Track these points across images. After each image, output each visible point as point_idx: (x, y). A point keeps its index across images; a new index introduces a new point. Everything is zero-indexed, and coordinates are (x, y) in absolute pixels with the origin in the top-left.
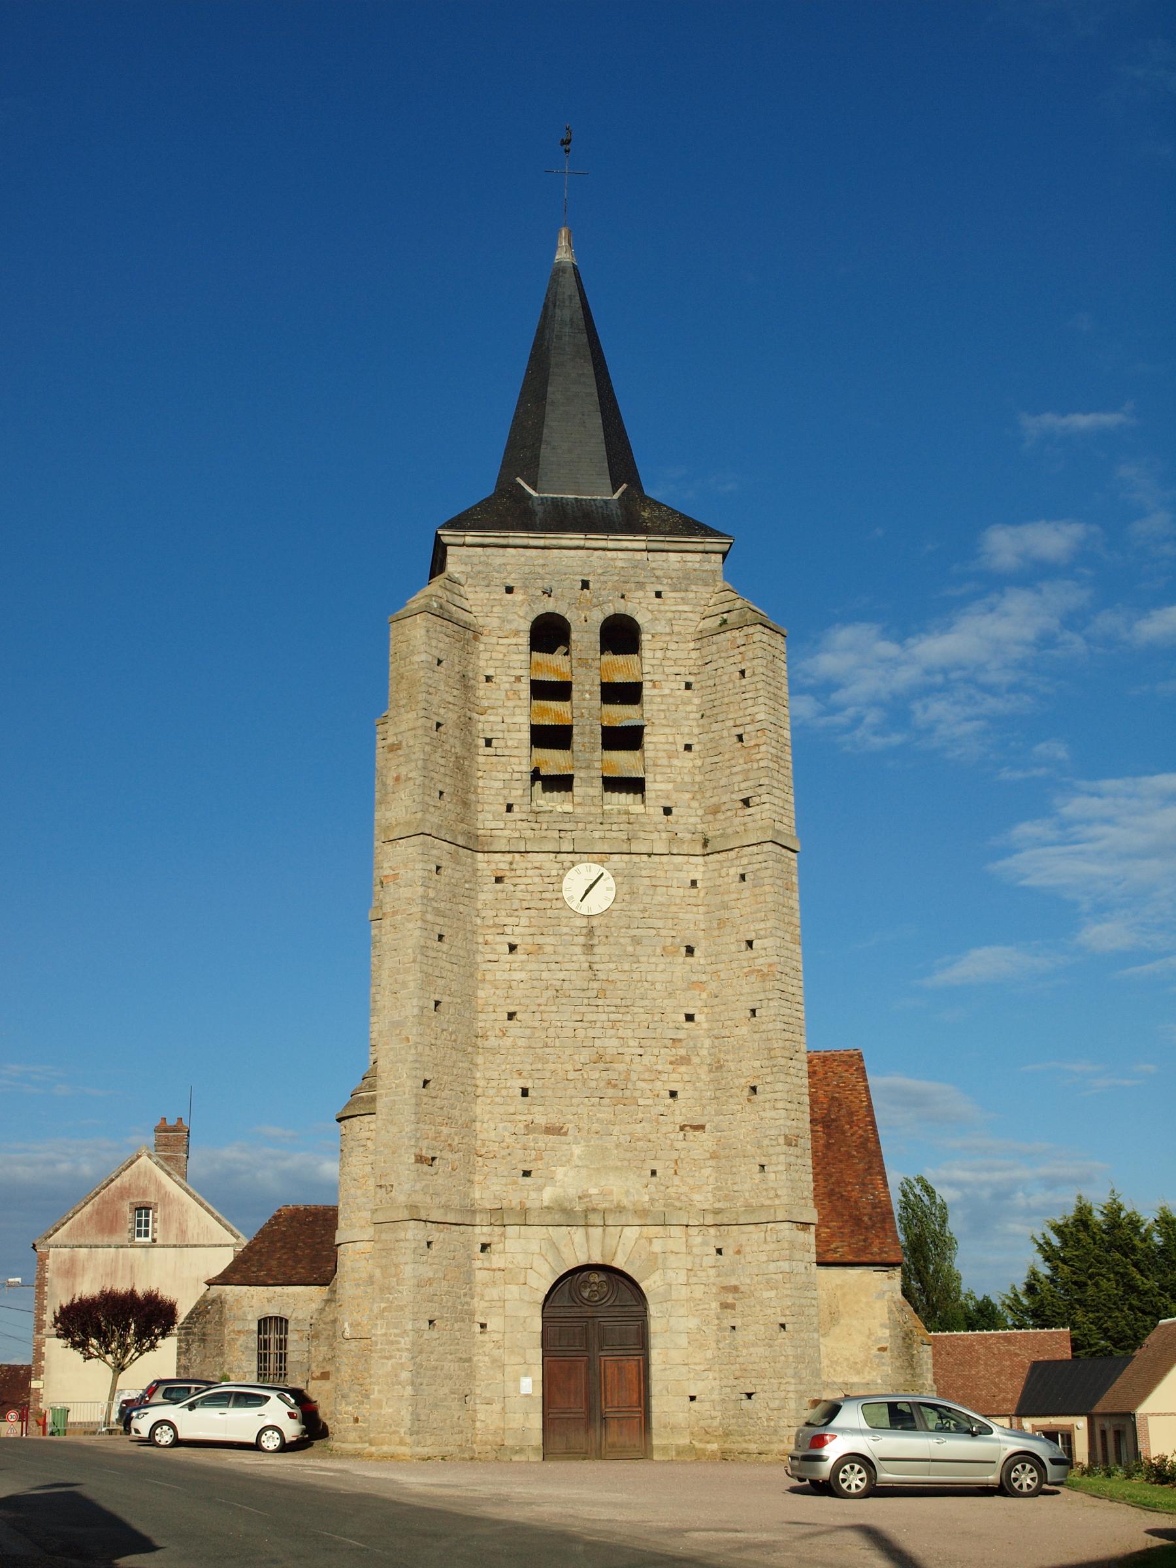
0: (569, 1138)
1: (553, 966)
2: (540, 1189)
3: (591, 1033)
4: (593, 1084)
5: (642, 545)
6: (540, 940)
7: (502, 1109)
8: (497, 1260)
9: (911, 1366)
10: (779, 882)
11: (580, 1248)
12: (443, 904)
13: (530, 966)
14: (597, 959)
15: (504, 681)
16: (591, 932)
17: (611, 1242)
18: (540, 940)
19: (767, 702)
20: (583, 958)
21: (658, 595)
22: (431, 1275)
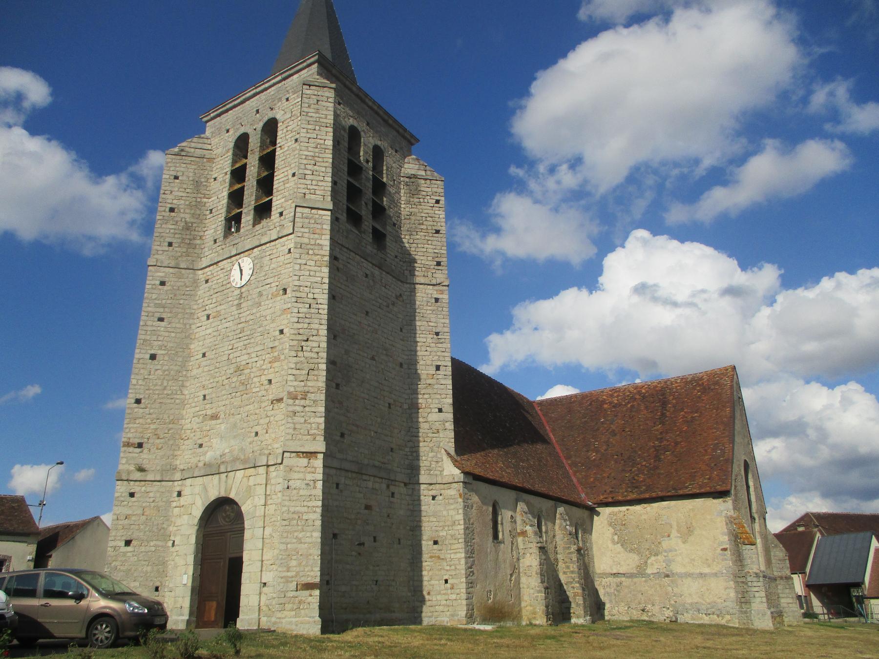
0: (219, 421)
1: (224, 321)
2: (205, 454)
3: (236, 355)
4: (233, 385)
5: (279, 78)
6: (219, 308)
7: (193, 410)
8: (183, 500)
9: (741, 561)
10: (306, 230)
11: (214, 489)
12: (164, 301)
13: (213, 325)
14: (242, 311)
15: (220, 179)
16: (241, 296)
17: (230, 482)
18: (219, 308)
19: (306, 126)
20: (236, 312)
21: (287, 100)
22: (130, 512)
